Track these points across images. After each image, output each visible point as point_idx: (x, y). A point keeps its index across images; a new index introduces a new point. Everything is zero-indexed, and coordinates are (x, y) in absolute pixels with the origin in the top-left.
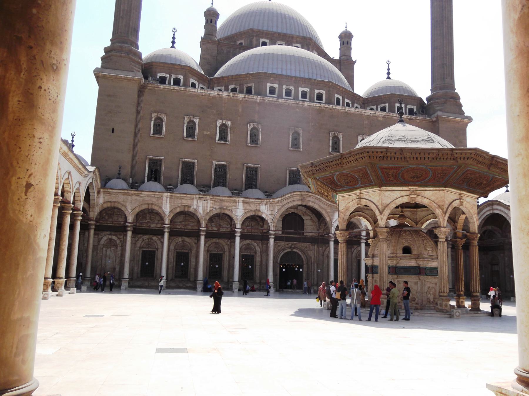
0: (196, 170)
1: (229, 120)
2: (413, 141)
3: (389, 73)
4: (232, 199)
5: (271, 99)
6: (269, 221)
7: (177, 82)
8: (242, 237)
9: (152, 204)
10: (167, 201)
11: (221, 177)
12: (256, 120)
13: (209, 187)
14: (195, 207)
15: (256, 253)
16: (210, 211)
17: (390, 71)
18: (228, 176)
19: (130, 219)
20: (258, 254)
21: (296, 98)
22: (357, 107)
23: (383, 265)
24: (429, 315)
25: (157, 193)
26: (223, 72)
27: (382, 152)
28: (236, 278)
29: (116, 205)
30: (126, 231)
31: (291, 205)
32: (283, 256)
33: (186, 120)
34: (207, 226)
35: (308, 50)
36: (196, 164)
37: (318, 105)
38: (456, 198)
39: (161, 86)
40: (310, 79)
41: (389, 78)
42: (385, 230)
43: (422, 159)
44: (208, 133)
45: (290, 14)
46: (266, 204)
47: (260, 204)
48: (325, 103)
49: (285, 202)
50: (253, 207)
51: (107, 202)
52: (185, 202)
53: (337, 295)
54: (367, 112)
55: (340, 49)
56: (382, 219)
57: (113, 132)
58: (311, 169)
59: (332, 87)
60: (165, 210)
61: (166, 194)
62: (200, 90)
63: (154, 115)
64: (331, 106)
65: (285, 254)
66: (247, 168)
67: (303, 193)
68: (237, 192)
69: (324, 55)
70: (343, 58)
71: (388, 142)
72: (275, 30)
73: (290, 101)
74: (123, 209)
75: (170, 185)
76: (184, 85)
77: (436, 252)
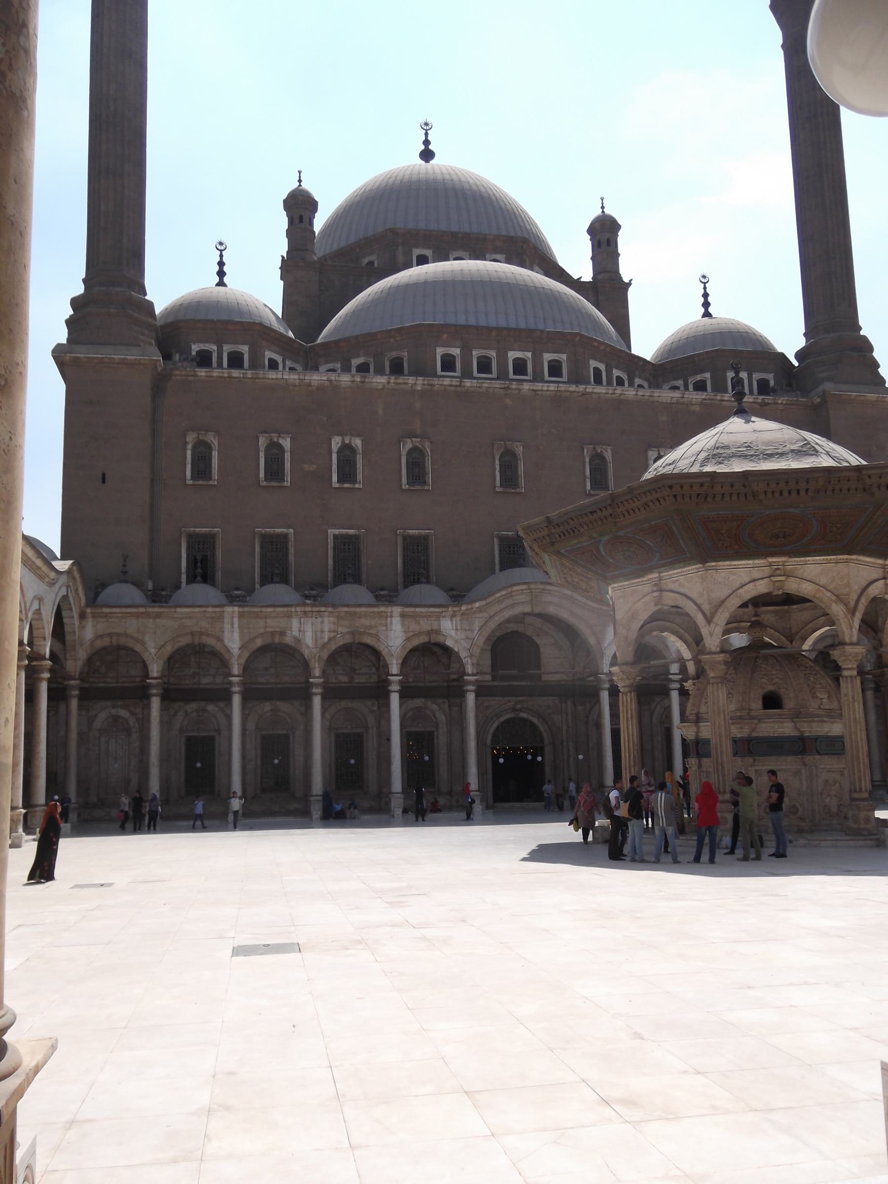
0: (291, 550)
1: (358, 435)
2: (771, 455)
3: (706, 305)
4: (376, 610)
5: (447, 381)
6: (463, 654)
7: (236, 361)
9: (201, 634)
10: (232, 624)
11: (348, 563)
13: (325, 587)
14: (295, 633)
16: (330, 639)
17: (710, 299)
18: (363, 560)
19: (155, 670)
20: (443, 729)
21: (502, 375)
22: (640, 386)
23: (720, 736)
24: (830, 843)
25: (210, 609)
26: (337, 329)
27: (702, 485)
28: (397, 785)
29: (123, 641)
30: (148, 697)
31: (507, 614)
32: (497, 729)
33: (263, 442)
34: (324, 673)
35: (522, 265)
36: (292, 538)
37: (553, 387)
38: (874, 576)
39: (202, 372)
40: (530, 331)
41: (707, 314)
42: (721, 657)
43: (794, 494)
44: (313, 467)
45: (474, 187)
46: (453, 616)
47: (438, 617)
48: (569, 382)
49: (496, 608)
50: (425, 625)
51: (101, 636)
52: (273, 624)
53: (623, 811)
54: (665, 395)
55: (592, 258)
56: (711, 635)
57: (104, 481)
58: (547, 532)
59: (582, 345)
60: (229, 645)
61: (229, 609)
62: (287, 375)
63: (191, 438)
64: (581, 388)
65: (502, 724)
66: (405, 538)
67: (532, 586)
68: (385, 595)
69: (560, 275)
70: (600, 277)
71: (714, 461)
72: (443, 227)
73: (490, 384)
74: (138, 648)
75: (237, 589)
76: (253, 366)
77: (839, 701)
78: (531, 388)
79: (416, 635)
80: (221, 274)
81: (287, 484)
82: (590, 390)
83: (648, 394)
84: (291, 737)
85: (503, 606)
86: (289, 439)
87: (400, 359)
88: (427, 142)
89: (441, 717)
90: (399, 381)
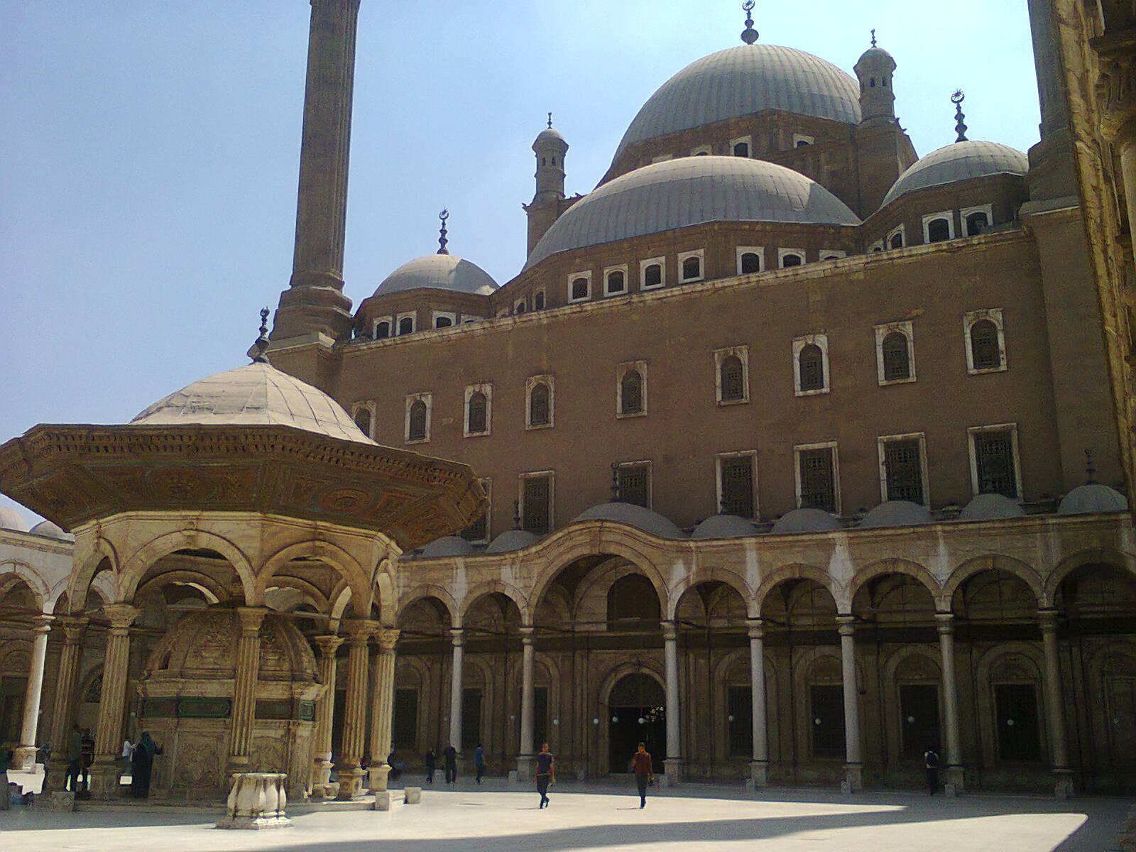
1: (484, 383)
3: (961, 128)
6: (520, 605)
8: (468, 649)
12: (545, 368)
17: (965, 122)
21: (634, 289)
33: (409, 403)
41: (962, 138)
46: (513, 564)
47: (500, 565)
48: (706, 279)
49: (555, 552)
50: (486, 575)
65: (620, 682)
67: (589, 525)
73: (613, 301)
78: (654, 297)
79: (478, 587)
80: (443, 241)
81: (427, 440)
82: (720, 285)
83: (791, 273)
84: (419, 693)
85: (562, 549)
86: (430, 396)
87: (542, 293)
90: (524, 319)
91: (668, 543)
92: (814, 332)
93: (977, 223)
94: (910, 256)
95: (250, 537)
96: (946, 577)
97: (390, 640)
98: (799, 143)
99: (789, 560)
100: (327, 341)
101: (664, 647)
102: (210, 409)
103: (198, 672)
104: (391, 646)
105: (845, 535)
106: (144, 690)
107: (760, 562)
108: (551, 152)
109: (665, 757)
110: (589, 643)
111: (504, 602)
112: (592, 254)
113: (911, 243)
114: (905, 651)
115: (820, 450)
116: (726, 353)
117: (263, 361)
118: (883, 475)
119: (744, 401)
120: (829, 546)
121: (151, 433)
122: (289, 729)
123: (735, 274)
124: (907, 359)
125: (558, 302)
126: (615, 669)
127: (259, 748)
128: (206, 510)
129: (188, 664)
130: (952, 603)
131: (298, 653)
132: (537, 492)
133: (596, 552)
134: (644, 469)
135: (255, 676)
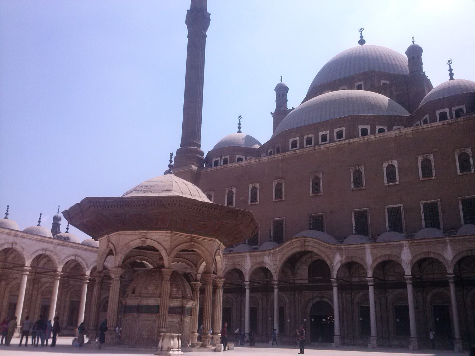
1: (257, 183)
3: (451, 75)
6: (273, 272)
8: (252, 290)
15: (285, 305)
17: (453, 72)
21: (317, 144)
33: (227, 191)
41: (452, 79)
46: (269, 255)
48: (346, 139)
50: (259, 260)
64: (356, 140)
65: (314, 305)
66: (275, 222)
73: (308, 149)
79: (255, 264)
80: (239, 128)
82: (352, 141)
85: (289, 249)
87: (279, 147)
88: (361, 37)
89: (287, 300)
91: (333, 246)
92: (392, 159)
93: (460, 112)
94: (431, 127)
95: (166, 240)
96: (451, 259)
97: (221, 283)
98: (384, 84)
99: (385, 253)
100: (194, 168)
101: (332, 290)
102: (151, 191)
103: (146, 295)
104: (221, 286)
105: (407, 242)
106: (125, 302)
107: (372, 254)
108: (282, 92)
109: (334, 335)
110: (301, 288)
111: (265, 271)
112: (299, 131)
113: (431, 122)
114: (435, 291)
115: (396, 208)
116: (355, 168)
117: (171, 173)
118: (423, 217)
119: (363, 188)
120: (401, 247)
121: (129, 200)
122: (181, 319)
123: (358, 137)
124: (431, 170)
125: (285, 150)
126: (312, 299)
127: (170, 326)
128: (150, 230)
129: (142, 292)
130: (454, 270)
131: (185, 288)
132: (278, 226)
133: (303, 250)
134: (322, 216)
135: (168, 297)
